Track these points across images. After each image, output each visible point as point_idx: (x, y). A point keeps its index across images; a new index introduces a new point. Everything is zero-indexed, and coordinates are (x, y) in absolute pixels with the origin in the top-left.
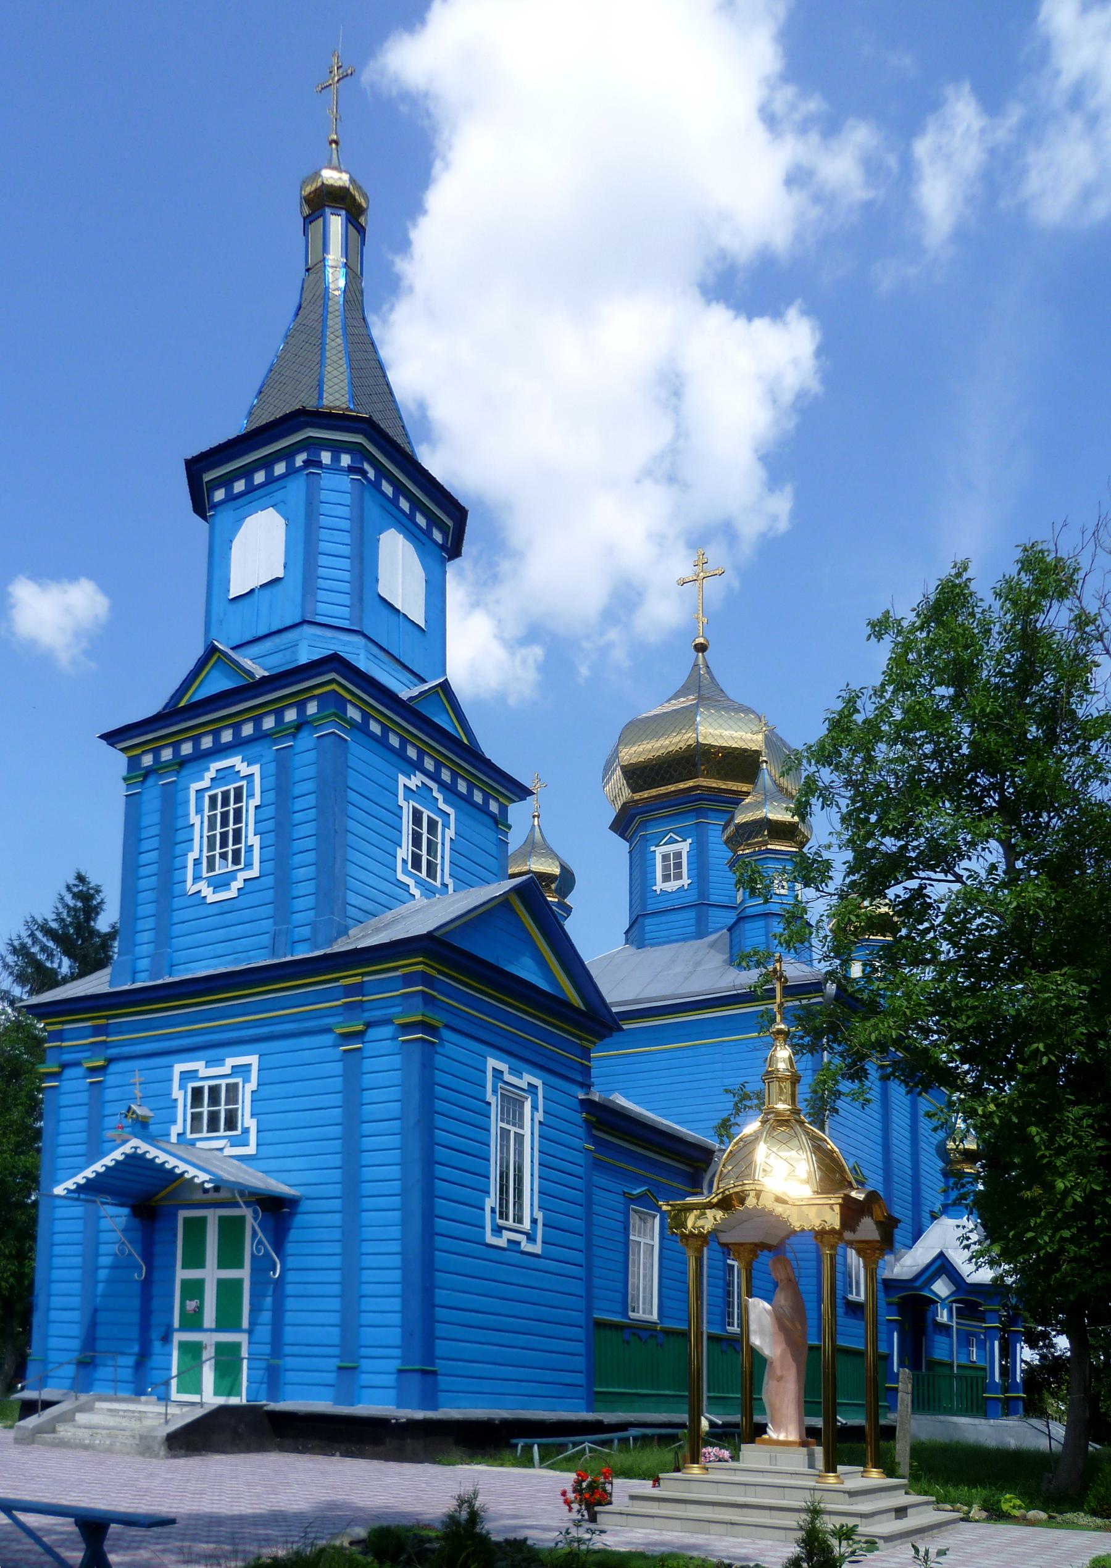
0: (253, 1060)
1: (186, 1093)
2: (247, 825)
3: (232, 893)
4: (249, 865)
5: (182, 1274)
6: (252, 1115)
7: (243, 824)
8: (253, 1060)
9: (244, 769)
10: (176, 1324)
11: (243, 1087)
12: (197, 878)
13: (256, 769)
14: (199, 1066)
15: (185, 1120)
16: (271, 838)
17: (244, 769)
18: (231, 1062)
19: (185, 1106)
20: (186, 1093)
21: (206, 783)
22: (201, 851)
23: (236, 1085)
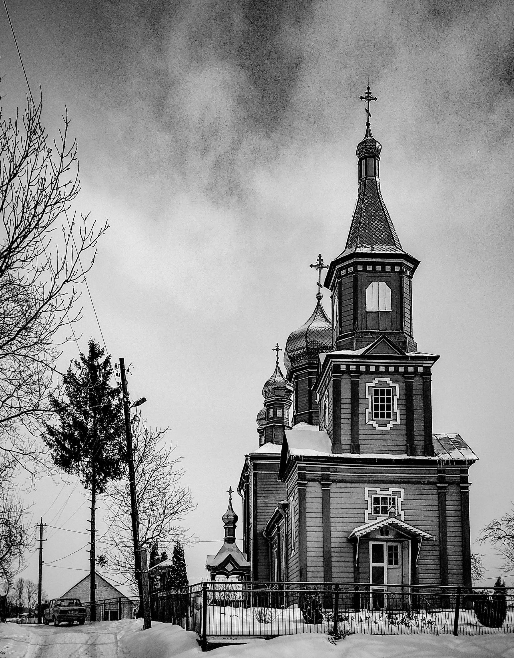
0: (402, 490)
1: (371, 499)
2: (393, 404)
3: (388, 428)
4: (396, 420)
5: (372, 565)
6: (402, 510)
7: (392, 404)
8: (402, 490)
9: (391, 384)
10: (371, 583)
11: (398, 499)
12: (370, 420)
13: (397, 385)
14: (378, 489)
15: (371, 509)
16: (404, 412)
17: (391, 384)
18: (391, 490)
19: (371, 503)
20: (371, 499)
21: (373, 384)
22: (372, 409)
23: (394, 499)
